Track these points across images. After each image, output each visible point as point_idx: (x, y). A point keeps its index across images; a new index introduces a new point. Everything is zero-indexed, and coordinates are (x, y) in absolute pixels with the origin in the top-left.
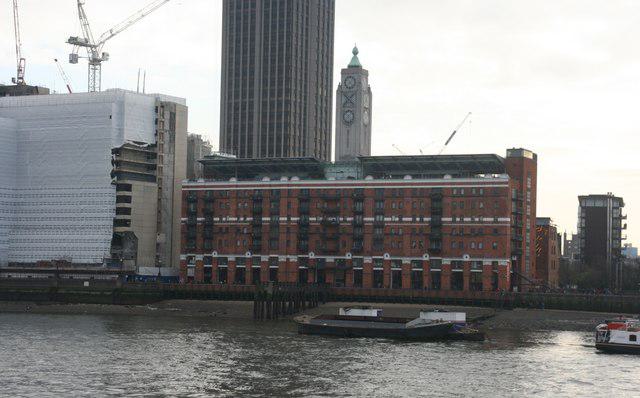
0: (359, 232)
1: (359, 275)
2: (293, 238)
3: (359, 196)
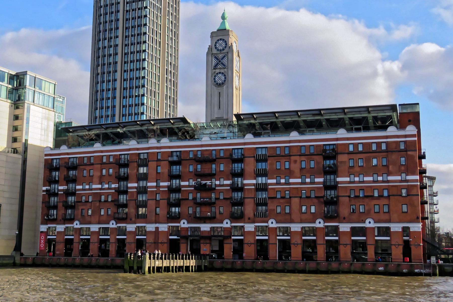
0: (238, 195)
2: (164, 203)
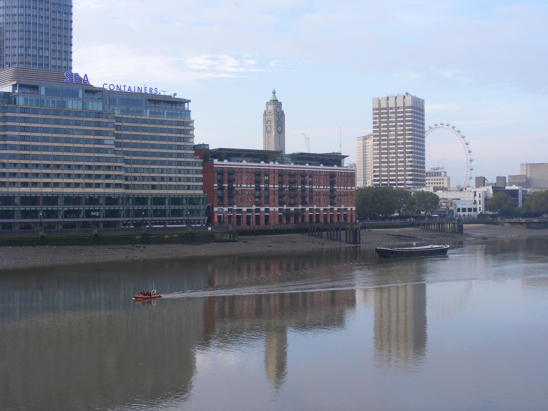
1: (303, 217)
2: (277, 197)
3: (303, 174)
